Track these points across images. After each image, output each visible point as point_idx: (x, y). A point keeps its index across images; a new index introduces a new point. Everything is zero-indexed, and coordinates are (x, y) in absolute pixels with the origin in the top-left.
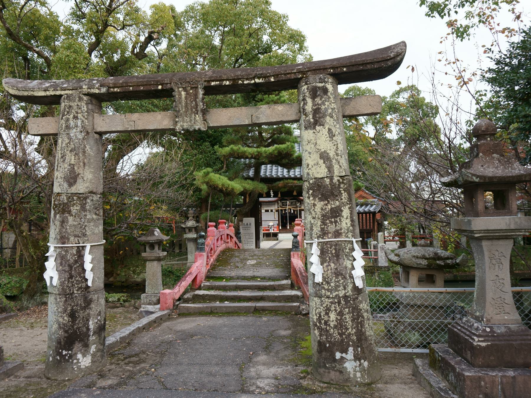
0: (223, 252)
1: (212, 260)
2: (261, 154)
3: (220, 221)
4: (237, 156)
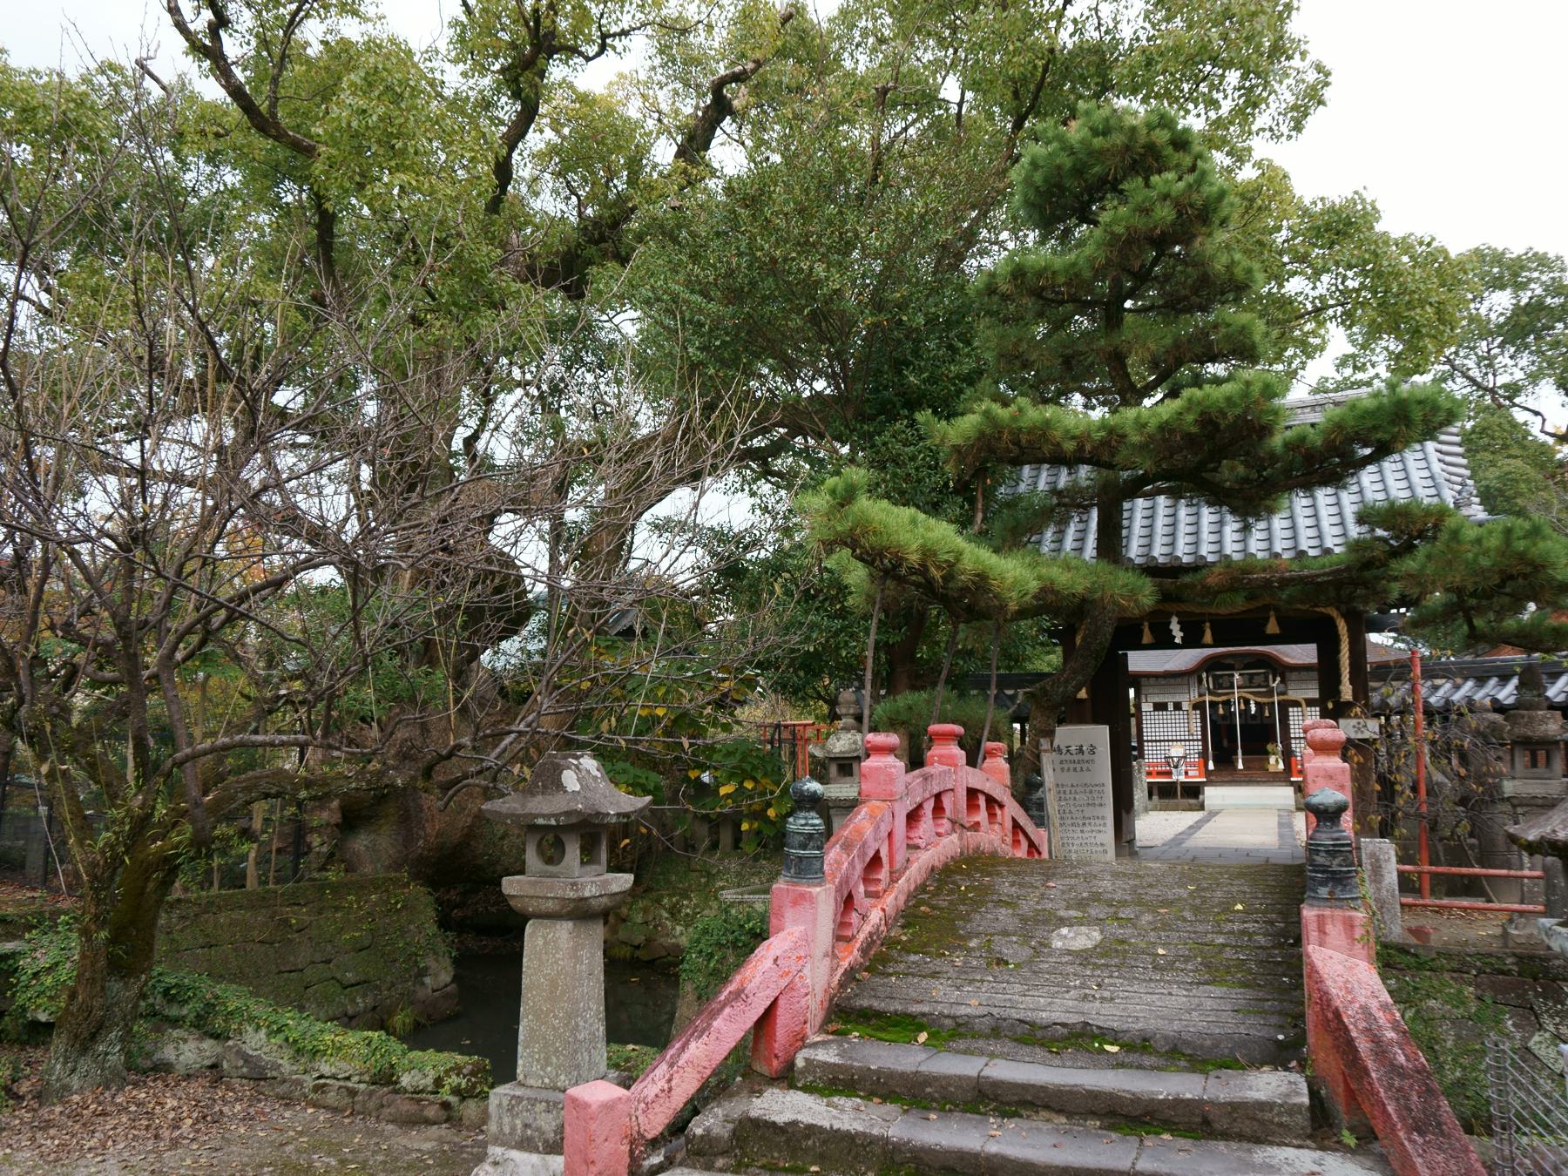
0: (944, 875)
1: (875, 916)
2: (1124, 436)
3: (935, 728)
4: (1016, 451)
